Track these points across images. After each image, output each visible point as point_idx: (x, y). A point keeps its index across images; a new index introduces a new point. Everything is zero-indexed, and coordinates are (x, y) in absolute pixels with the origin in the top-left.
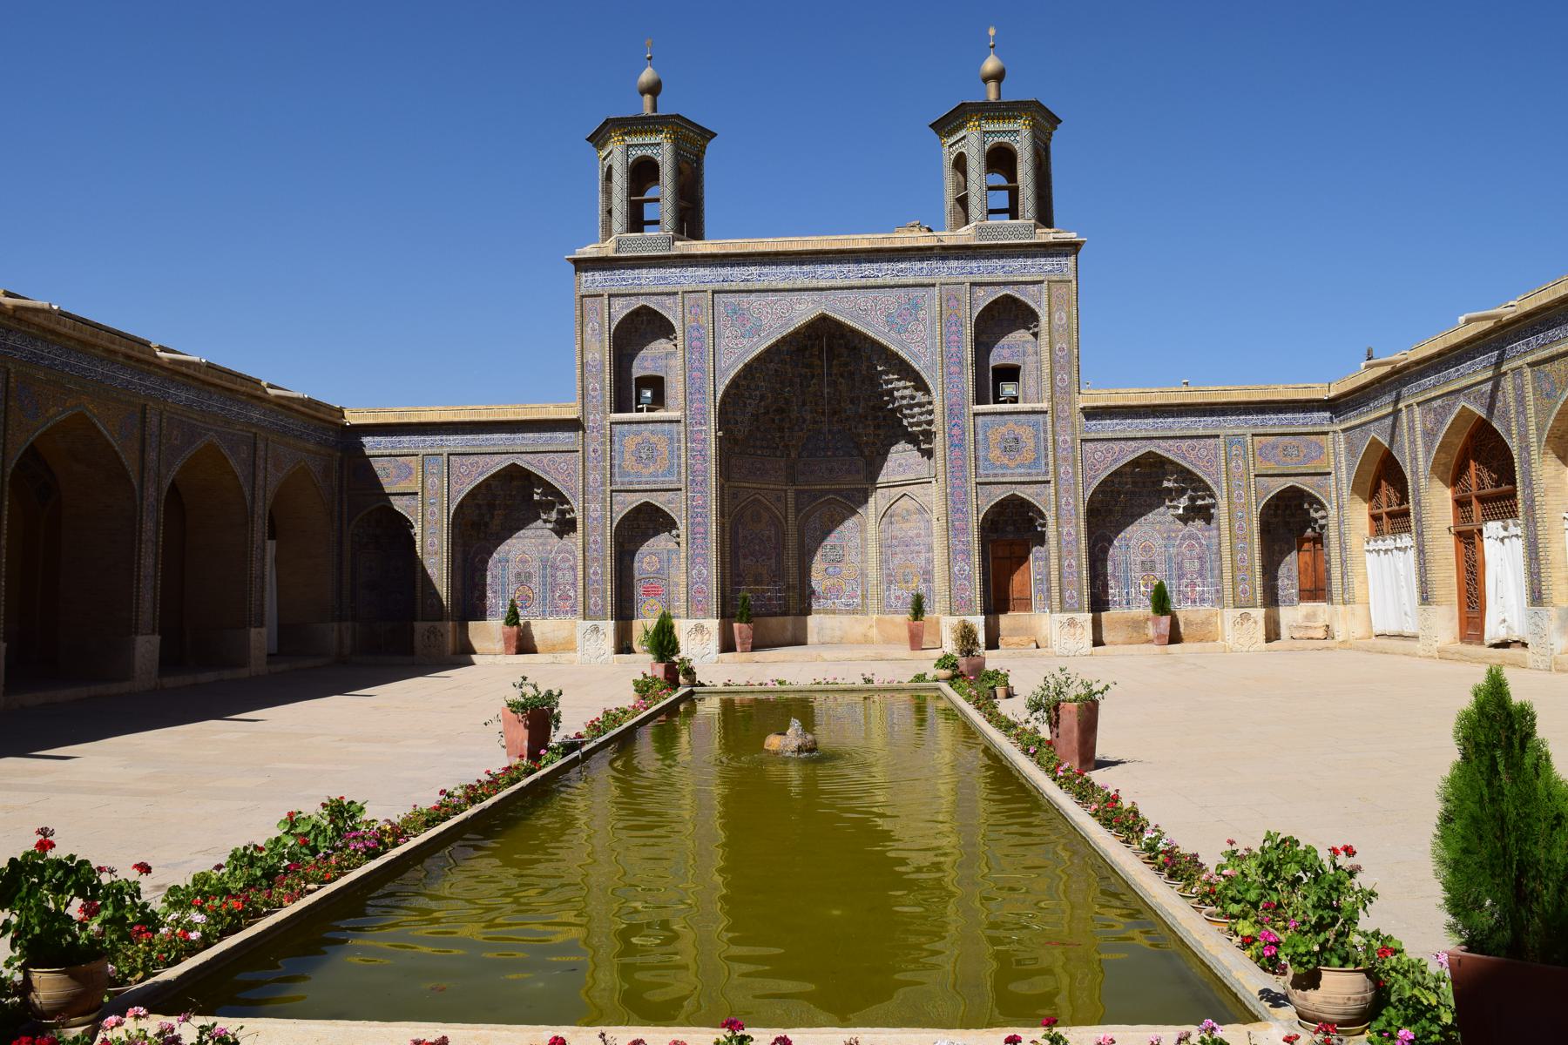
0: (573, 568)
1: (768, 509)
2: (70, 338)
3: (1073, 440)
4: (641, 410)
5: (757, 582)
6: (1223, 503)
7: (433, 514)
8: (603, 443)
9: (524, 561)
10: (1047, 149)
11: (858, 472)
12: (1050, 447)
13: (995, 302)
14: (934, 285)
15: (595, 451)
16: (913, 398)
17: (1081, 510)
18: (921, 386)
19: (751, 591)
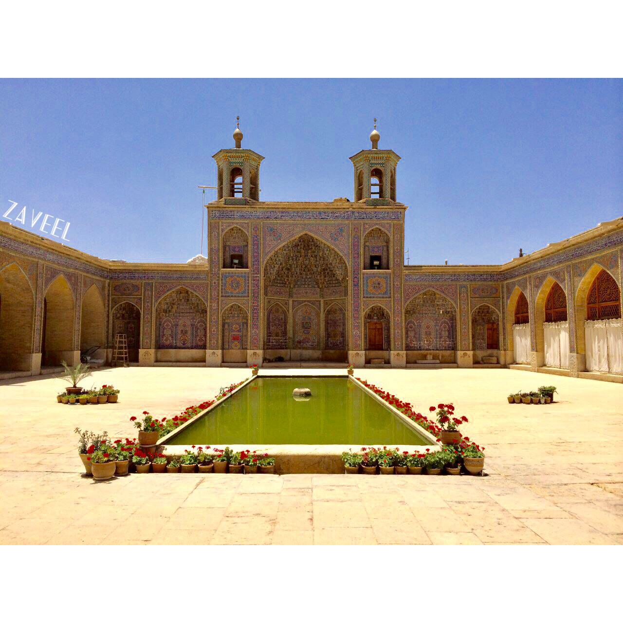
0: (205, 329)
1: (281, 307)
2: (11, 235)
4: (233, 268)
5: (277, 336)
6: (458, 310)
7: (148, 306)
8: (218, 280)
9: (184, 326)
10: (395, 169)
12: (392, 287)
13: (373, 230)
15: (215, 283)
17: (403, 311)
19: (275, 339)
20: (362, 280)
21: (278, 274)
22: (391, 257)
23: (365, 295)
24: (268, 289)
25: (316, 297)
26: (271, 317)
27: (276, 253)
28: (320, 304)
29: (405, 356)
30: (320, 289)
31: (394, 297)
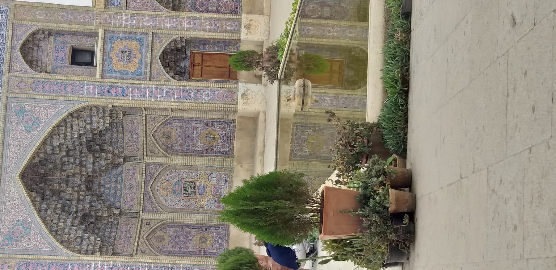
1: (154, 231)
3: (127, 15)
5: (205, 241)
11: (134, 168)
13: (24, 58)
14: (7, 97)
16: (85, 121)
17: (173, 13)
18: (76, 115)
20: (115, 81)
21: (93, 233)
22: (74, 27)
23: (142, 77)
24: (119, 251)
25: (139, 169)
26: (171, 249)
27: (55, 233)
28: (154, 164)
29: (250, 17)
31: (149, 27)
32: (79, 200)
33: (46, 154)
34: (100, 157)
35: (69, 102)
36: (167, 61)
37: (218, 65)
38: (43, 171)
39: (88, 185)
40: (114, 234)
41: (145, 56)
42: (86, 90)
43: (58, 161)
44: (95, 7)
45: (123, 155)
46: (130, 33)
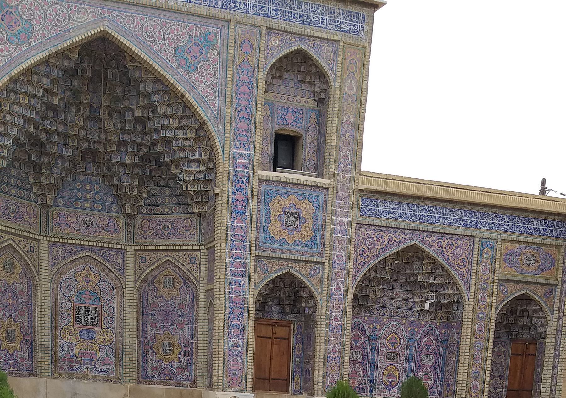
30: (127, 216)
32: (65, 136)
33: (138, 82)
34: (132, 177)
35: (222, 122)
36: (281, 284)
37: (273, 361)
38: (110, 77)
39: (91, 156)
40: (13, 191)
41: (290, 250)
42: (240, 154)
43: (126, 103)
44: (361, 175)
45: (136, 213)
46: (324, 229)
